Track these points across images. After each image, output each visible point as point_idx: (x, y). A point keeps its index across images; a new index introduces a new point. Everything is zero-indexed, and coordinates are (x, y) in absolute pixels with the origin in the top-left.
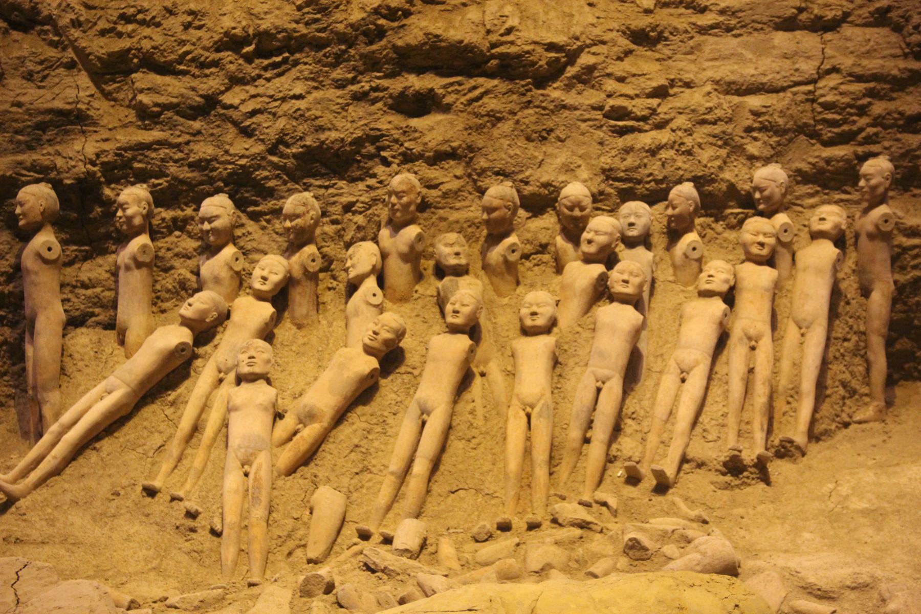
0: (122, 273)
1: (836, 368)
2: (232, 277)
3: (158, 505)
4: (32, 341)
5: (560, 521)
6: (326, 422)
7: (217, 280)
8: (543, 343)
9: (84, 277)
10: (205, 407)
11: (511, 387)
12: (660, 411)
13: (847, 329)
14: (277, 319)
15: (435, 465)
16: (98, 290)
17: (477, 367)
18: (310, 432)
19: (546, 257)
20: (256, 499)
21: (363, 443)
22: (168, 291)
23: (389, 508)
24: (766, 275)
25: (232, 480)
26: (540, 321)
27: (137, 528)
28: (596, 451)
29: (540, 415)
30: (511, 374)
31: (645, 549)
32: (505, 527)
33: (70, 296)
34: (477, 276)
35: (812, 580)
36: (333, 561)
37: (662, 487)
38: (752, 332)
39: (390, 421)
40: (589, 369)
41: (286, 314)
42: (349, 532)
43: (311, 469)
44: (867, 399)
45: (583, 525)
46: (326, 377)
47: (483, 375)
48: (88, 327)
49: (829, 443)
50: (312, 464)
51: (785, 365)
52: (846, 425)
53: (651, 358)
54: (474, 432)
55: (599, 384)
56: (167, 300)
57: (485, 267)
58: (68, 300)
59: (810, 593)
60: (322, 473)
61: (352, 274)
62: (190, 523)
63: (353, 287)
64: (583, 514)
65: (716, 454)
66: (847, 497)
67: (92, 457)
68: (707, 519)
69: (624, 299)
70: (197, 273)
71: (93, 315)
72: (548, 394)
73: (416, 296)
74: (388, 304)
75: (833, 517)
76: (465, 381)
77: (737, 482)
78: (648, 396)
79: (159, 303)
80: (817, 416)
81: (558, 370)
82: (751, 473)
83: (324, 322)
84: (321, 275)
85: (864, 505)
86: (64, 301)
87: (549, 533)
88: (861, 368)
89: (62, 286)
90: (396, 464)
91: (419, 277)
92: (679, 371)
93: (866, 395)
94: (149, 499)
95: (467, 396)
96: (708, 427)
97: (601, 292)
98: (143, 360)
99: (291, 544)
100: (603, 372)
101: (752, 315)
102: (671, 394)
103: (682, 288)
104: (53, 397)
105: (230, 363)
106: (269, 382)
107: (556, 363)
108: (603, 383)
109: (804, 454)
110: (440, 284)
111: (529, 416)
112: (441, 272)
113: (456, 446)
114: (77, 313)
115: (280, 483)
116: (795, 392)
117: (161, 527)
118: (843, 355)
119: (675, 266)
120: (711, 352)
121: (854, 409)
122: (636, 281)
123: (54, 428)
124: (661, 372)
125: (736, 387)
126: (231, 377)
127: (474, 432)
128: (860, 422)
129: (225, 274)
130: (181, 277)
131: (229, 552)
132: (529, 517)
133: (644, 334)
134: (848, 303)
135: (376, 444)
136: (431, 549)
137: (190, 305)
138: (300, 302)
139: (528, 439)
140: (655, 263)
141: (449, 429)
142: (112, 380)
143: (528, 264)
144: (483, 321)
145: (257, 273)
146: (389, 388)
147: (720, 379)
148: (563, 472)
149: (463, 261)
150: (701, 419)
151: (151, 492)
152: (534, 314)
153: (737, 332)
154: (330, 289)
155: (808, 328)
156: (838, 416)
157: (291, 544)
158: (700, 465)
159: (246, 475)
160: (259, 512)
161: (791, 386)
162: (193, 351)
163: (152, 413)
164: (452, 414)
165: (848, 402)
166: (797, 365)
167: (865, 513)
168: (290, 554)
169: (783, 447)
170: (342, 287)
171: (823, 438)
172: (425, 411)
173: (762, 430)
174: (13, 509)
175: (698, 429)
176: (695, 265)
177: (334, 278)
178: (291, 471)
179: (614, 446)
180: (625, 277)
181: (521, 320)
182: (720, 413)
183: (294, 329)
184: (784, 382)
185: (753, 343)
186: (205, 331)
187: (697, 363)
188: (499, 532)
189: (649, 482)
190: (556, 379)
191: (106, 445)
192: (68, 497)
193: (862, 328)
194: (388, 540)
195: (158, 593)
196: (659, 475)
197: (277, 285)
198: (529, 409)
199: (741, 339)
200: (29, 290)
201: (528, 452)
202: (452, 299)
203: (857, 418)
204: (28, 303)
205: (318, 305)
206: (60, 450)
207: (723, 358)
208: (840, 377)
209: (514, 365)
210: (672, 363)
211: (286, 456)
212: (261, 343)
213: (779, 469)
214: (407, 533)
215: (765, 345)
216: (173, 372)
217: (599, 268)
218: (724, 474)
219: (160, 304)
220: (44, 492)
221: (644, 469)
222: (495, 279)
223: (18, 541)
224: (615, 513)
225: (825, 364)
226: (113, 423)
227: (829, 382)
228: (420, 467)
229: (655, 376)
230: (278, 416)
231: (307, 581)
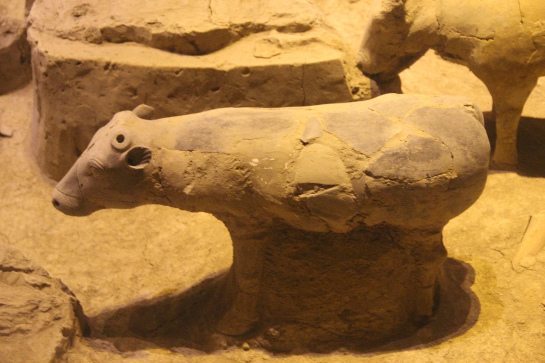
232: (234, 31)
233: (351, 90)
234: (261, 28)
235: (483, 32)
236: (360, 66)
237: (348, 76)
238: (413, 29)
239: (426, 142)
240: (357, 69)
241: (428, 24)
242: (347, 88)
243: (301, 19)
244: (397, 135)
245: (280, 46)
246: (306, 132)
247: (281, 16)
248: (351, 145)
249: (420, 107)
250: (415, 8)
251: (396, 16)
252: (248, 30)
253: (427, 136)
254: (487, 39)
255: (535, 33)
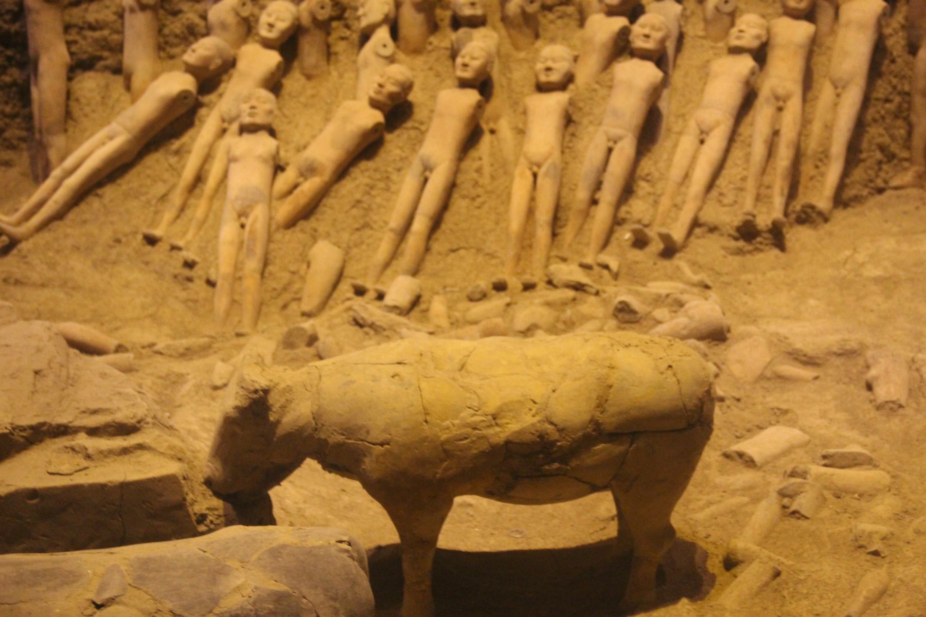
0: (127, 15)
1: (875, 133)
2: (239, 23)
3: (157, 254)
4: (36, 84)
5: (555, 282)
6: (327, 176)
7: (224, 26)
8: (557, 100)
9: (91, 17)
10: (208, 158)
11: (520, 144)
12: (676, 173)
13: (890, 89)
14: (285, 68)
15: (436, 223)
16: (106, 32)
17: (487, 123)
18: (310, 186)
19: (570, 9)
20: (251, 252)
21: (366, 198)
22: (176, 36)
23: (387, 265)
24: (803, 29)
25: (228, 231)
26: (555, 77)
27: (136, 275)
28: (603, 213)
29: (546, 174)
30: (521, 132)
31: (634, 312)
32: (500, 287)
33: (77, 38)
34: (495, 28)
35: (799, 345)
36: (325, 316)
37: (669, 251)
38: (781, 92)
39: (394, 177)
40: (603, 128)
41: (296, 64)
42: (345, 288)
43: (312, 223)
44: (906, 164)
45: (578, 287)
46: (331, 128)
47: (492, 132)
48: (97, 71)
49: (859, 209)
50: (313, 219)
51: (816, 127)
52: (880, 191)
53: (672, 119)
54: (480, 191)
55: (611, 144)
56: (177, 45)
57: (504, 19)
58: (75, 42)
59: (796, 359)
60: (322, 228)
61: (364, 23)
62: (187, 272)
63: (365, 37)
64: (580, 277)
65: (730, 218)
66: (862, 265)
67: (93, 204)
68: (709, 283)
69: (645, 55)
70: (204, 17)
71: (100, 58)
72: (557, 154)
73: (429, 48)
74: (401, 56)
75: (843, 284)
76: (472, 136)
77: (749, 247)
78: (665, 156)
79: (166, 48)
80: (848, 181)
81: (571, 129)
82: (765, 238)
83: (335, 74)
84: (335, 24)
85: (878, 272)
86: (69, 44)
87: (543, 294)
88: (903, 132)
89: (67, 28)
90: (395, 220)
91: (433, 27)
92: (698, 132)
93: (906, 160)
94: (148, 248)
95: (473, 154)
96: (725, 191)
97: (621, 47)
98: (144, 108)
99: (287, 296)
100: (616, 132)
101: (783, 73)
102: (688, 154)
103: (712, 44)
104: (58, 142)
105: (234, 113)
106: (272, 133)
107: (568, 120)
108: (615, 142)
109: (826, 220)
110: (453, 36)
111: (535, 175)
112: (457, 23)
113: (459, 204)
114: (85, 56)
115: (278, 236)
116: (824, 156)
117: (160, 275)
118: (883, 118)
119: (706, 21)
120: (734, 112)
121: (891, 174)
122: (657, 35)
123: (56, 173)
124: (680, 133)
125: (759, 149)
126: (235, 127)
127: (480, 191)
128: (896, 188)
129: (231, 19)
130: (190, 22)
131: (221, 302)
132: (527, 278)
133: (665, 93)
134: (893, 61)
135: (378, 200)
136: (423, 306)
137: (194, 51)
138: (310, 52)
139: (532, 199)
140: (684, 16)
141: (451, 188)
142: (114, 126)
143: (551, 16)
144: (496, 74)
145: (264, 19)
146: (395, 143)
147: (743, 142)
148: (568, 233)
149: (479, 12)
150: (717, 183)
151: (151, 241)
152: (548, 69)
153: (765, 92)
154: (343, 39)
155: (844, 87)
156: (871, 181)
157: (287, 296)
158: (713, 229)
159: (243, 226)
160: (252, 265)
161: (821, 149)
162: (197, 99)
163: (156, 161)
164: (456, 172)
165: (885, 167)
166: (828, 127)
167: (877, 280)
168: (285, 307)
169: (805, 212)
170: (355, 37)
171: (852, 204)
172: (428, 167)
173: (782, 194)
174: (15, 251)
175: (714, 193)
176: (727, 20)
177: (348, 27)
178: (291, 224)
179: (624, 209)
180: (647, 31)
181: (536, 76)
182: (739, 177)
183: (303, 80)
184: (812, 145)
185: (781, 104)
186: (210, 79)
187: (718, 124)
188: (494, 292)
189: (657, 246)
190: (567, 138)
191: (109, 192)
192: (70, 242)
193: (907, 88)
194: (380, 296)
195: (148, 338)
196: (666, 238)
197: (283, 33)
198: (535, 169)
199: (767, 100)
200: (31, 30)
201: (531, 212)
202: (463, 52)
203: (895, 182)
204: (32, 44)
205: (329, 54)
206: (62, 195)
207: (748, 119)
208: (879, 140)
209: (525, 123)
210: (692, 124)
211: (284, 210)
212: (265, 94)
213: (798, 236)
214: (400, 289)
215: (794, 106)
216: (176, 120)
217: (620, 22)
218: (736, 239)
219: (168, 49)
220: (46, 236)
221: (652, 233)
222: (512, 32)
223: (18, 282)
224: (616, 276)
225: (860, 126)
226: (115, 170)
227: (865, 145)
228: (420, 225)
229: (673, 136)
230: (279, 168)
231: (289, 334)
232: (18, 437)
233: (194, 518)
234: (63, 431)
235: (376, 435)
236: (208, 482)
237: (190, 497)
238: (280, 431)
239: (279, 597)
240: (204, 487)
241: (301, 423)
242: (189, 516)
243: (123, 415)
244: (238, 588)
245: (88, 457)
246: (102, 588)
247: (95, 412)
248: (169, 605)
249: (274, 545)
250: (283, 400)
251: (255, 412)
252: (40, 434)
253: (282, 587)
254: (382, 445)
255: (444, 437)
